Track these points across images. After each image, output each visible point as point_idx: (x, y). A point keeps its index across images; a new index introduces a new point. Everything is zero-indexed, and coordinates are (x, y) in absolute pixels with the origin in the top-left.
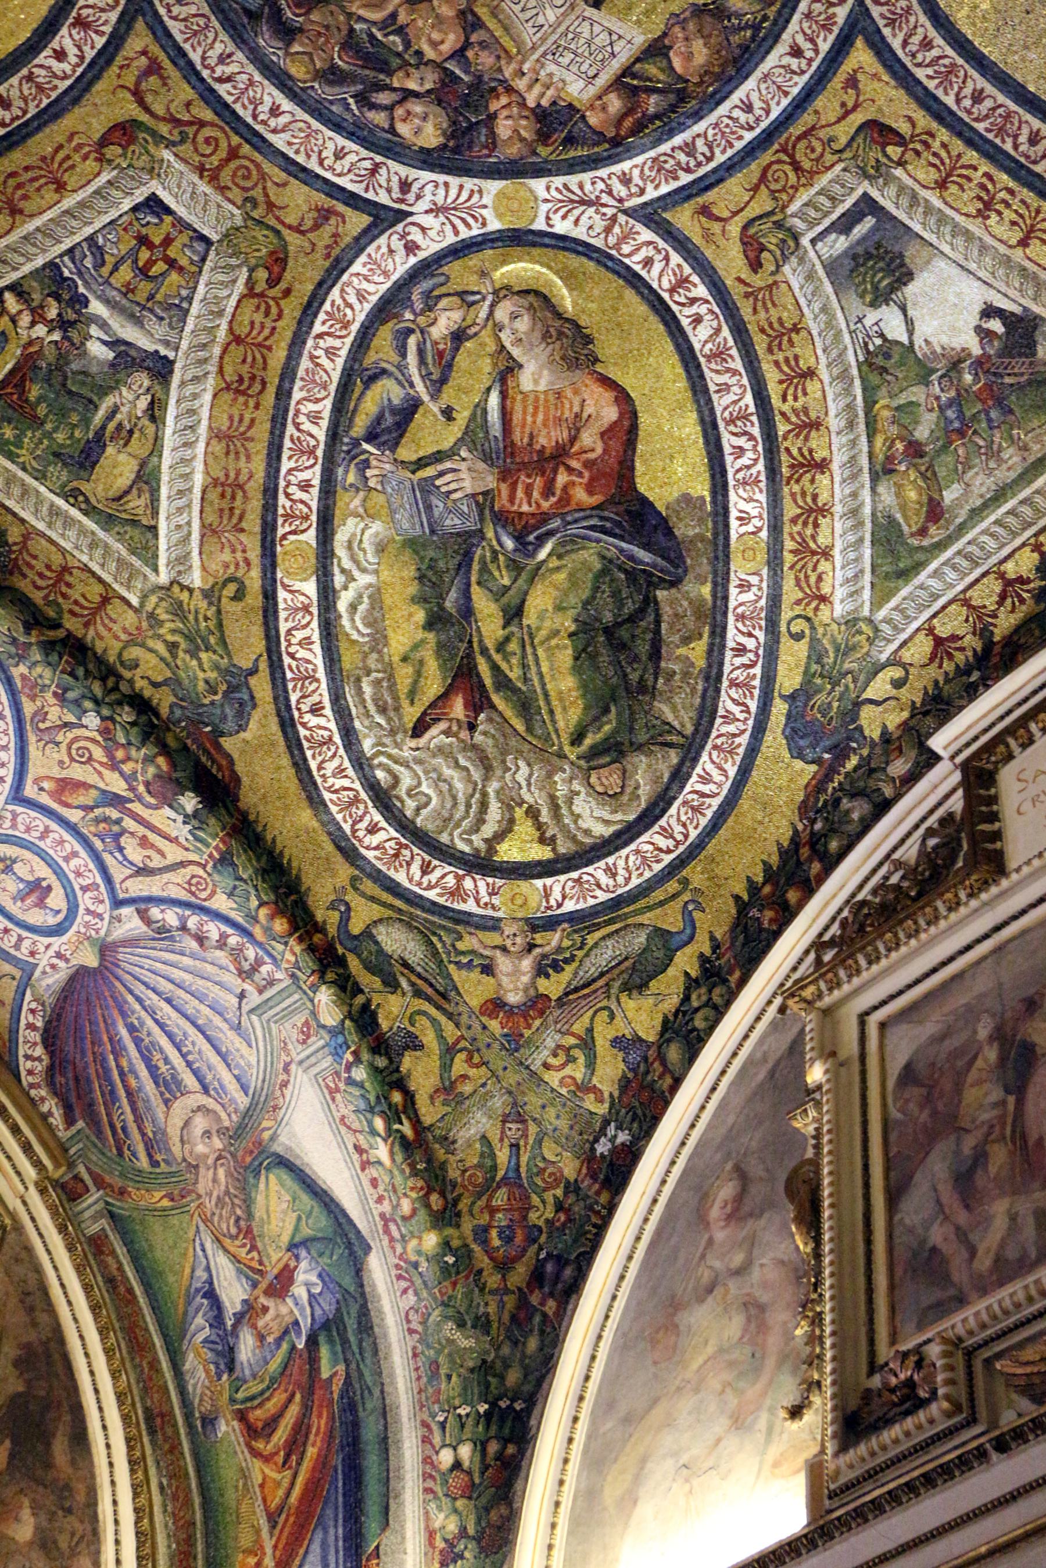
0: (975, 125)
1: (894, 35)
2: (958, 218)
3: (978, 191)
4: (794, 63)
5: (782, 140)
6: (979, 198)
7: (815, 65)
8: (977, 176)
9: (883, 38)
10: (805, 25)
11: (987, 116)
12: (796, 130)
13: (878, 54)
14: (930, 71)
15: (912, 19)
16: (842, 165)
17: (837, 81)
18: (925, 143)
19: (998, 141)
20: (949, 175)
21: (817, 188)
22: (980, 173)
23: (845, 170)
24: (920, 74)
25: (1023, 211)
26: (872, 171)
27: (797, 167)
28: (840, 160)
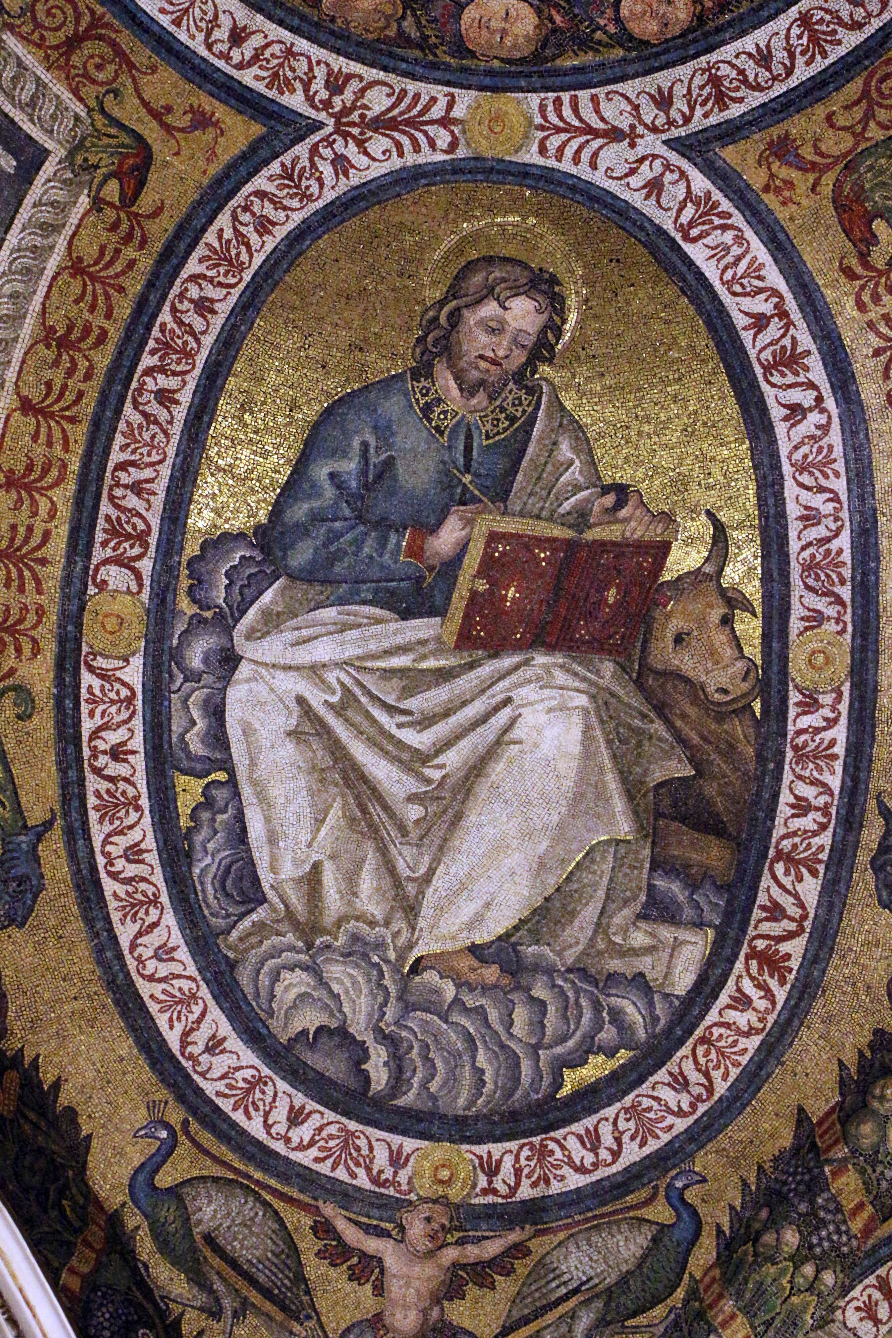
0: (167, 308)
1: (270, 179)
2: (38, 298)
3: (80, 323)
4: (222, 34)
5: (108, 18)
6: (70, 329)
7: (221, 64)
8: (97, 321)
9: (267, 162)
10: (276, 49)
11: (180, 323)
12: (126, 39)
13: (243, 157)
14: (228, 234)
15: (295, 203)
16: (83, 114)
17: (208, 104)
18: (128, 238)
19: (151, 344)
20: (93, 278)
21: (46, 77)
22: (106, 325)
23: (77, 118)
24: (223, 220)
25: (70, 397)
26: (79, 160)
27: (72, 43)
28: (90, 110)
